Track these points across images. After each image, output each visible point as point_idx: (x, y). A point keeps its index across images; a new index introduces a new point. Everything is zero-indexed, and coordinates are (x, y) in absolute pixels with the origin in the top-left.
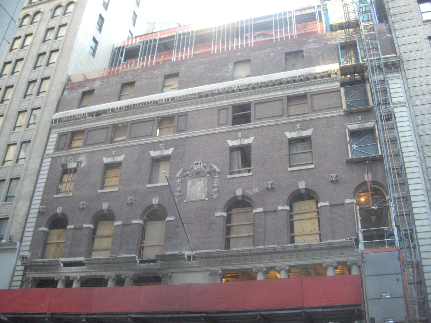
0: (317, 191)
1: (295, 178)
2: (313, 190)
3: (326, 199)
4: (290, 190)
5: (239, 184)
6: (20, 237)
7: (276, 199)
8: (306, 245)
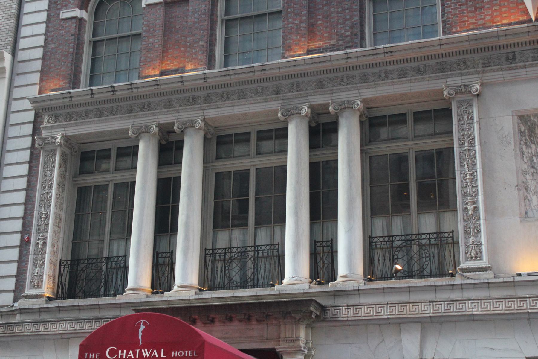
6: (10, 39)
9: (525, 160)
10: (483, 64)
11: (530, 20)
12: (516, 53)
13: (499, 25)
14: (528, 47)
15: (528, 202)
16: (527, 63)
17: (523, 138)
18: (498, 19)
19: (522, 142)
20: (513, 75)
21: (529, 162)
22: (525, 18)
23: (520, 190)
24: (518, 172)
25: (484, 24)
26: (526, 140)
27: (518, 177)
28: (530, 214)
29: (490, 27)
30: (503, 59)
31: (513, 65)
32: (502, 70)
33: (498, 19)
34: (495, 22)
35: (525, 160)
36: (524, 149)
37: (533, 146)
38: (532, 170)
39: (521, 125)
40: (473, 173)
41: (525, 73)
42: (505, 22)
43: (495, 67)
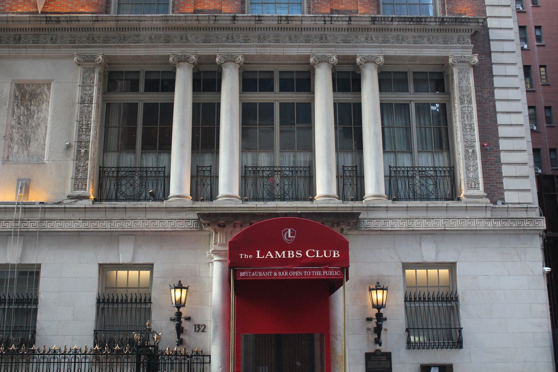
8: (281, 17)
9: (15, 118)
10: (70, 41)
11: (37, 12)
12: (22, 36)
13: (14, 12)
14: (31, 33)
15: (10, 150)
16: (27, 45)
17: (16, 101)
18: (14, 8)
19: (15, 104)
20: (17, 52)
21: (17, 120)
22: (34, 10)
23: (6, 140)
24: (7, 126)
25: (4, 10)
26: (18, 103)
27: (6, 130)
28: (11, 158)
29: (8, 13)
30: (11, 39)
31: (17, 45)
32: (8, 47)
33: (14, 8)
34: (12, 10)
35: (15, 118)
36: (16, 110)
37: (22, 108)
38: (18, 126)
39: (16, 91)
40: (88, 124)
41: (25, 52)
42: (19, 10)
43: (4, 44)
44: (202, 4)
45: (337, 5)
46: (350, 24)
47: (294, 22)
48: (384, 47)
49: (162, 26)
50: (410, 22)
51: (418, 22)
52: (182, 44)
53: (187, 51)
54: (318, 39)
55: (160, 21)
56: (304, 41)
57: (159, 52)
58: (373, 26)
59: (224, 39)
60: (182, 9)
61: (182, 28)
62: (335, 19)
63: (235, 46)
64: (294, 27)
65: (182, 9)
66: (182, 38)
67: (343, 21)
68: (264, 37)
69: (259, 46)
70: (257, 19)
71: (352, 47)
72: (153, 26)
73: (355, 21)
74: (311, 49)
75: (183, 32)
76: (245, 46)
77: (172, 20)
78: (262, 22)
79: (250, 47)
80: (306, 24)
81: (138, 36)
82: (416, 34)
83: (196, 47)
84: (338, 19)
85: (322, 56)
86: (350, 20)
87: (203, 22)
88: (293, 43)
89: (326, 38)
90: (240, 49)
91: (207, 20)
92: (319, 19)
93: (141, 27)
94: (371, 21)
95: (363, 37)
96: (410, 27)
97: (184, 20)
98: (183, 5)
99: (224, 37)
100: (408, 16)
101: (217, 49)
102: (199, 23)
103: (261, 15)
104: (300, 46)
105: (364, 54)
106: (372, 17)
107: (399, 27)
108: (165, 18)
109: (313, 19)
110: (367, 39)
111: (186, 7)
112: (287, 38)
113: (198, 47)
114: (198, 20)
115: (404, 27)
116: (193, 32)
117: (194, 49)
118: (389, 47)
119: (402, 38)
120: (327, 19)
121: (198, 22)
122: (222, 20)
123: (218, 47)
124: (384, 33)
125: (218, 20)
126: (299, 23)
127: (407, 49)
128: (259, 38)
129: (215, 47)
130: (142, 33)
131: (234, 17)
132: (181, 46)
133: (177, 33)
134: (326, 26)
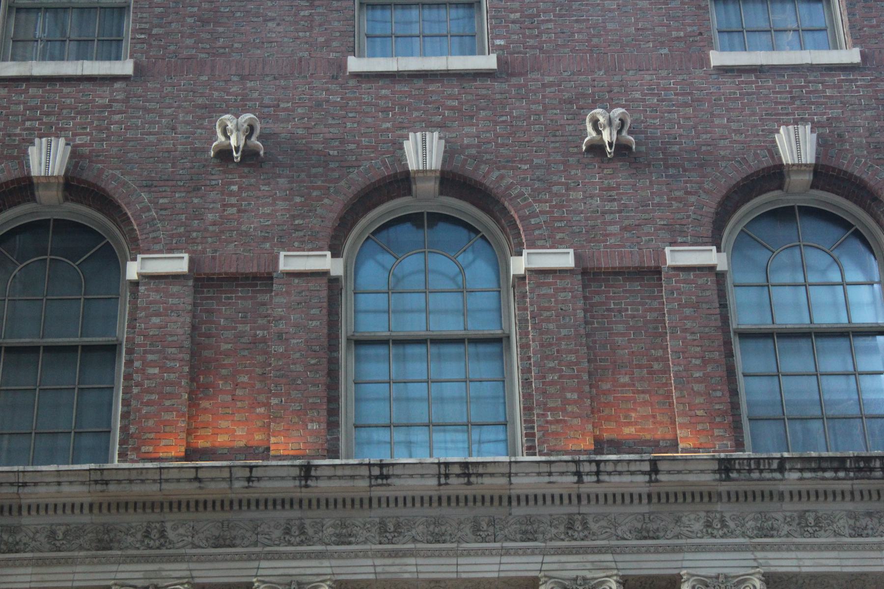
0: (509, 187)
1: (385, 110)
2: (487, 182)
3: (559, 236)
4: (354, 175)
5: (48, 114)
7: (267, 210)
8: (447, 464)
44: (209, 432)
45: (613, 425)
46: (657, 481)
47: (487, 480)
48: (763, 547)
49: (87, 500)
50: (836, 470)
51: (860, 470)
52: (147, 552)
53: (164, 573)
54: (562, 528)
55: (83, 483)
56: (518, 536)
57: (77, 577)
58: (724, 487)
59: (277, 533)
60: (151, 449)
61: (148, 505)
62: (610, 468)
63: (309, 556)
64: (488, 494)
65: (151, 449)
66: (147, 535)
67: (632, 473)
68: (398, 526)
69: (382, 554)
70: (376, 471)
71: (665, 552)
72: (60, 501)
73: (669, 472)
74: (539, 559)
75: (155, 517)
76: (340, 556)
77: (119, 482)
78: (389, 481)
79: (356, 557)
80: (523, 483)
81: (13, 530)
82: (861, 507)
83: (189, 559)
84: (619, 468)
85: (576, 579)
86: (654, 469)
87: (212, 485)
88: (484, 540)
89: (585, 525)
90: (326, 563)
91: (224, 479)
92: (563, 467)
93: (25, 502)
94: (719, 471)
95: (697, 520)
96: (839, 486)
97: (155, 481)
98: (152, 436)
99: (276, 527)
100: (831, 454)
101: (255, 564)
102: (200, 488)
103: (388, 460)
104: (507, 552)
105: (703, 572)
106: (720, 461)
107: (804, 487)
108: (97, 476)
109: (545, 468)
110: (708, 525)
111: (163, 443)
112: (467, 530)
113: (197, 561)
114: (197, 479)
115: (821, 486)
116: (184, 515)
117: (184, 566)
118: (779, 548)
119: (817, 519)
120: (586, 468)
121: (197, 484)
122: (270, 478)
123: (259, 557)
124: (759, 506)
125: (259, 479)
126: (504, 481)
127: (834, 554)
128: (383, 529)
129: (249, 558)
130: (26, 520)
131: (308, 468)
132: (147, 559)
133: (135, 519)
134: (584, 489)
